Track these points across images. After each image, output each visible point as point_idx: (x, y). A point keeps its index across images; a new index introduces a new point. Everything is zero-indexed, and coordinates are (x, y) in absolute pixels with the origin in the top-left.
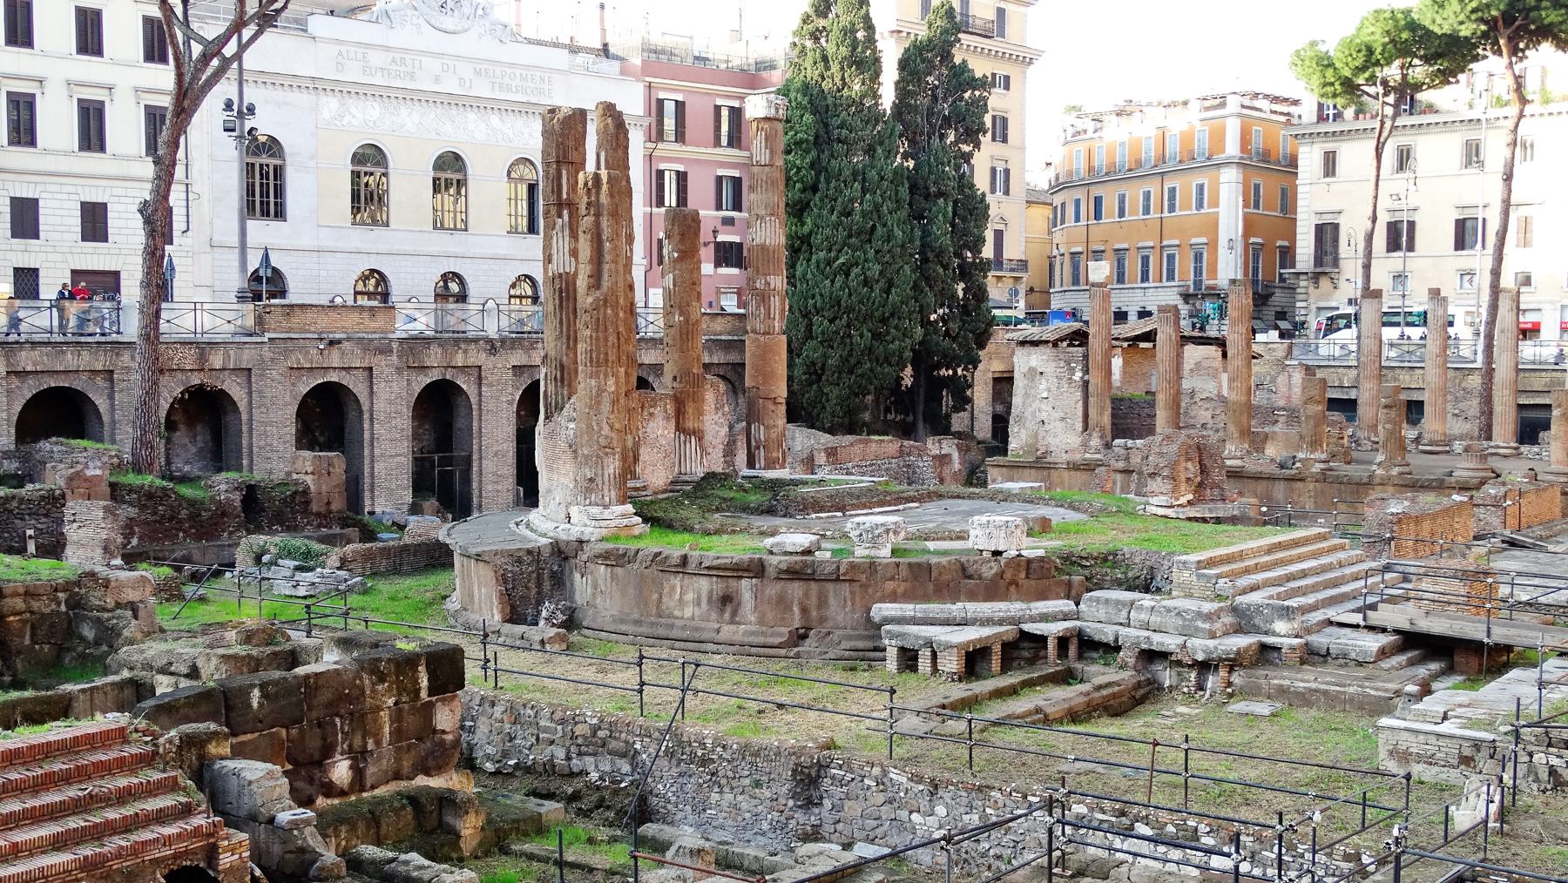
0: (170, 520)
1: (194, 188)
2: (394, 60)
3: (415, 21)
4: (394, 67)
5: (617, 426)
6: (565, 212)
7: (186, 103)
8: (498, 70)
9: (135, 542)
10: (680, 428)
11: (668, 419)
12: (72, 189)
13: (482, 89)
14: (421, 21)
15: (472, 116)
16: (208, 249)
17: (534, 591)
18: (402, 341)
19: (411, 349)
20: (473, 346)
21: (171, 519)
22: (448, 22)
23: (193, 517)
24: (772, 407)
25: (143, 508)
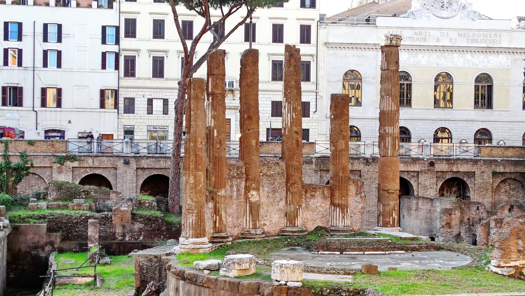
0: (158, 230)
1: (320, 94)
2: (416, 33)
3: (427, 15)
4: (416, 36)
5: (194, 200)
6: (210, 98)
7: (189, 60)
8: (471, 33)
9: (141, 238)
10: (332, 203)
11: (325, 198)
12: (268, 96)
13: (463, 43)
14: (430, 14)
15: (455, 55)
16: (325, 119)
17: (158, 275)
18: (317, 158)
19: (322, 162)
20: (356, 161)
21: (158, 230)
22: (445, 14)
23: (167, 229)
24: (387, 195)
25: (146, 224)
